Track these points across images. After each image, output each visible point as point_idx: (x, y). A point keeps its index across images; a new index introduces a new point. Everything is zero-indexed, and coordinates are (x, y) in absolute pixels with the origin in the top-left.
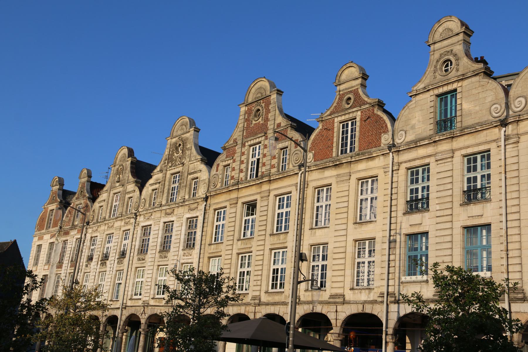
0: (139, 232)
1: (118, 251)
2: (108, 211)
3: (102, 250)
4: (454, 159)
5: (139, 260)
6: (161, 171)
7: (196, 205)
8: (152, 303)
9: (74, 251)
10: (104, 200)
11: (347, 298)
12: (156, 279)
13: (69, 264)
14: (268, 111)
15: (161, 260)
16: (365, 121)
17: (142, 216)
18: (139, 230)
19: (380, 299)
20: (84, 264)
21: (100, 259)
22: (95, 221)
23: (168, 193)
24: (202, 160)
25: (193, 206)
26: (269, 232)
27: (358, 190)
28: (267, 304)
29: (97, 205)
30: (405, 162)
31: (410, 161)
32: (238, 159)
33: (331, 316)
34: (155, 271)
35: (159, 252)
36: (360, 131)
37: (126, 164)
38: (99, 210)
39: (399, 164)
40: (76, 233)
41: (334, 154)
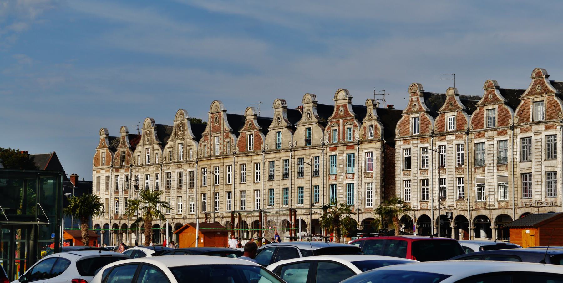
0: (165, 176)
1: (154, 186)
2: (144, 159)
3: (143, 184)
6: (172, 141)
10: (140, 152)
12: (177, 203)
13: (123, 192)
14: (221, 121)
15: (178, 193)
17: (165, 167)
18: (164, 174)
20: (134, 192)
22: (136, 165)
23: (178, 154)
24: (193, 139)
26: (225, 183)
27: (255, 168)
29: (135, 154)
32: (210, 143)
33: (247, 222)
34: (176, 199)
35: (177, 189)
37: (151, 130)
38: (138, 157)
39: (266, 159)
40: (124, 171)
41: (246, 150)
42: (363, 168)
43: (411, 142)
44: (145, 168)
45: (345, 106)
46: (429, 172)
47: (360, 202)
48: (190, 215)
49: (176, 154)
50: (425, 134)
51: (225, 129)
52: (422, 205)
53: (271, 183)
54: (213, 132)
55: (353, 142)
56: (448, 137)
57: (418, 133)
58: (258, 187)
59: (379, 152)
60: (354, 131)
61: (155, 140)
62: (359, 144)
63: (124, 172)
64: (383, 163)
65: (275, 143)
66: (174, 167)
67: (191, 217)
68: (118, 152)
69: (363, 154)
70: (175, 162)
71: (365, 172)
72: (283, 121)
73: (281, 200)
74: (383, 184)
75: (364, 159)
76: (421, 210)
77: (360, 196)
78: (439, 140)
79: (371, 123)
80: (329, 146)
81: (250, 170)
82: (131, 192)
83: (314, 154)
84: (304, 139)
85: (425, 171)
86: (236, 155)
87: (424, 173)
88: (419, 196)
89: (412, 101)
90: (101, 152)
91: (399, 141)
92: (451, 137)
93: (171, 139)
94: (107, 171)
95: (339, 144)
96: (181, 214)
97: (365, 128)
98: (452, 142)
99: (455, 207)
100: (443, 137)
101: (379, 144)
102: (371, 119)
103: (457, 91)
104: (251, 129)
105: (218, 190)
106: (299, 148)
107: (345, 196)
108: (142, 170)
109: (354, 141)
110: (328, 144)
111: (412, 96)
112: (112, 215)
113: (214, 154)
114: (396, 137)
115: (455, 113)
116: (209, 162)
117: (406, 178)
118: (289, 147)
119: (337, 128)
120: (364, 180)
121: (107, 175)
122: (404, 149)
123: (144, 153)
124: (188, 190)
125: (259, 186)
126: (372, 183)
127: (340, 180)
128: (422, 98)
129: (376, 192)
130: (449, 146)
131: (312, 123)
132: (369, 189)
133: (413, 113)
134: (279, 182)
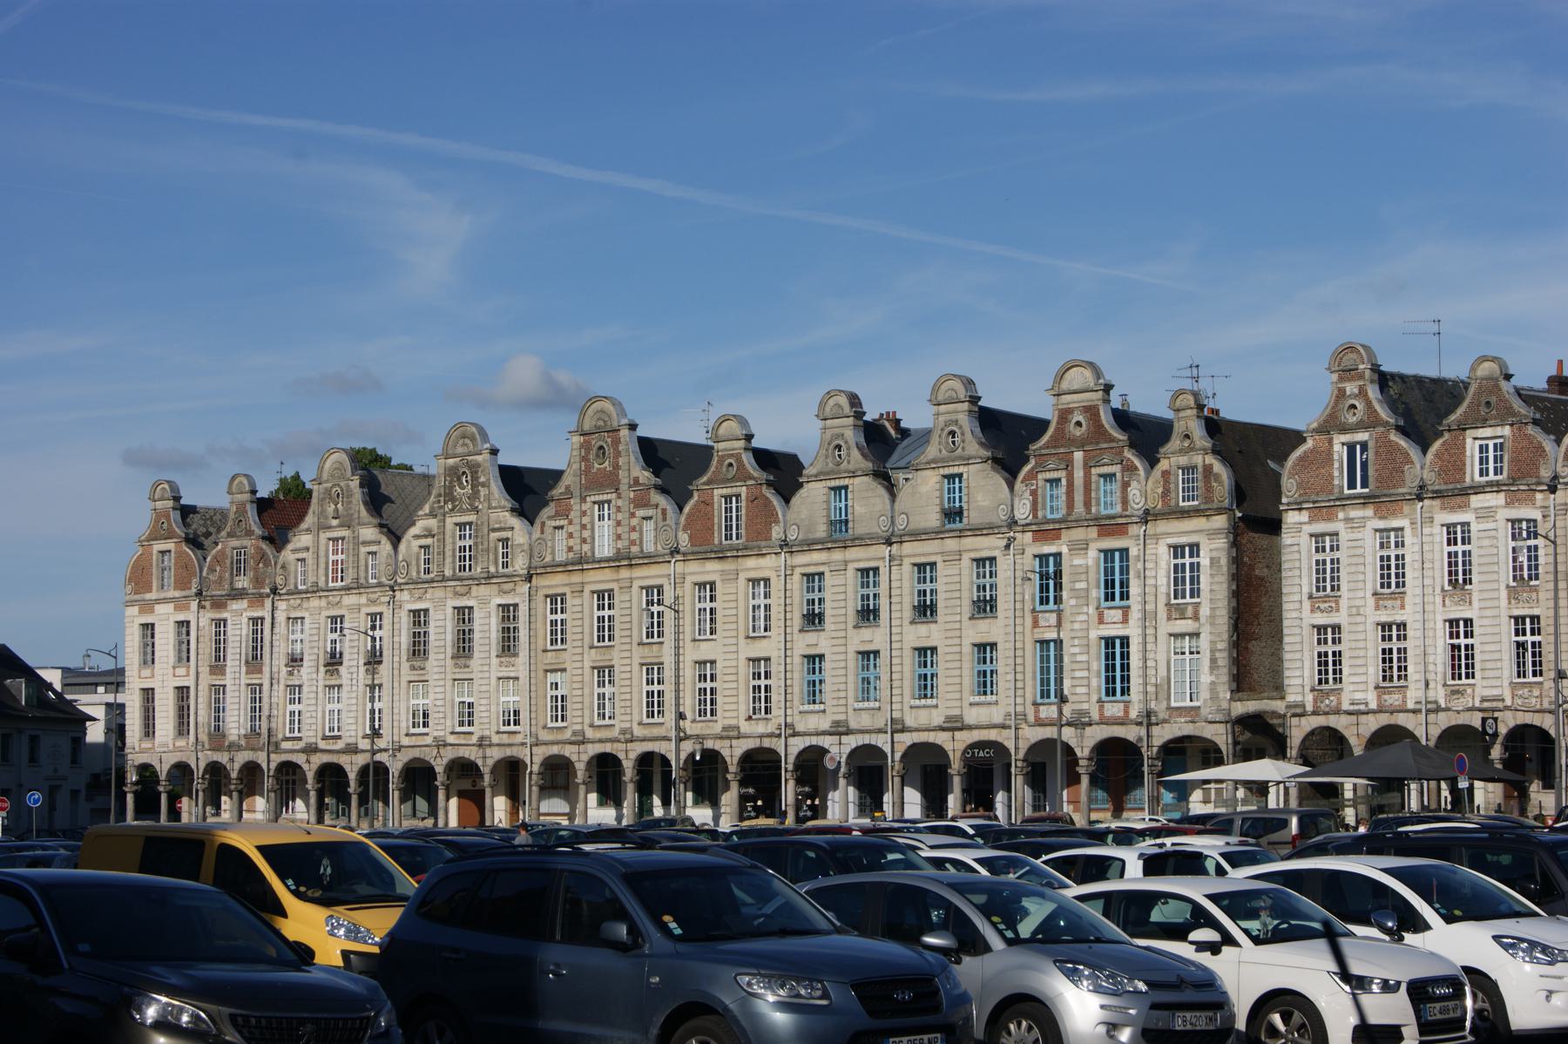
1: (362, 649)
2: (321, 571)
3: (321, 644)
4: (847, 572)
5: (413, 668)
6: (432, 514)
7: (511, 585)
8: (451, 739)
9: (247, 641)
11: (743, 730)
13: (244, 669)
14: (618, 454)
15: (458, 670)
16: (752, 501)
17: (406, 592)
19: (778, 732)
21: (322, 662)
22: (292, 587)
23: (454, 556)
24: (513, 510)
25: (507, 587)
26: (636, 640)
27: (748, 593)
28: (644, 740)
29: (288, 555)
30: (800, 566)
31: (804, 566)
32: (576, 521)
33: (725, 753)
34: (448, 688)
35: (452, 658)
36: (747, 515)
37: (348, 486)
39: (793, 567)
41: (716, 541)
42: (1163, 590)
43: (1341, 515)
44: (327, 596)
45: (1091, 411)
46: (1408, 599)
47: (1151, 689)
48: (505, 736)
49: (448, 554)
50: (1392, 491)
51: (636, 481)
52: (1386, 697)
53: (811, 637)
54: (587, 489)
55: (1121, 517)
56: (1476, 501)
57: (1363, 486)
58: (759, 649)
59: (1222, 543)
60: (1126, 485)
61: (364, 513)
62: (1146, 522)
63: (245, 610)
64: (1233, 574)
65: (825, 520)
66: (439, 593)
67: (506, 742)
68: (222, 552)
69: (1162, 552)
70: (444, 579)
71: (1168, 604)
72: (855, 453)
73: (851, 686)
74: (1235, 638)
75: (1163, 564)
76: (1380, 711)
77: (1151, 672)
78: (1443, 508)
79: (1190, 459)
80: (1034, 528)
81: (734, 600)
82: (275, 669)
83: (976, 550)
84: (938, 509)
85: (1396, 599)
86: (679, 557)
87: (1389, 603)
88: (1374, 671)
89: (1341, 394)
90: (155, 552)
91: (1296, 512)
92: (1488, 500)
93: (427, 509)
94: (180, 605)
95: (1067, 522)
96: (471, 733)
97: (1166, 474)
98: (1496, 512)
99: (1508, 702)
100: (1459, 500)
101: (1220, 521)
102: (1191, 449)
103: (1507, 368)
104: (733, 479)
105: (610, 660)
106: (917, 535)
107: (1093, 674)
108: (315, 603)
109: (1127, 513)
110: (1028, 521)
111: (1341, 379)
112: (203, 737)
113: (593, 553)
114: (1284, 500)
115: (1507, 431)
116: (576, 578)
117: (1321, 619)
118: (881, 527)
119: (1062, 474)
120: (1165, 627)
121: (181, 617)
122: (1311, 535)
123: (322, 553)
124: (495, 661)
125: (770, 647)
126: (1195, 635)
127: (1077, 626)
128: (1377, 387)
129: (1213, 660)
130: (1482, 527)
131: (967, 460)
132: (1183, 653)
133: (1344, 429)
134: (842, 634)
